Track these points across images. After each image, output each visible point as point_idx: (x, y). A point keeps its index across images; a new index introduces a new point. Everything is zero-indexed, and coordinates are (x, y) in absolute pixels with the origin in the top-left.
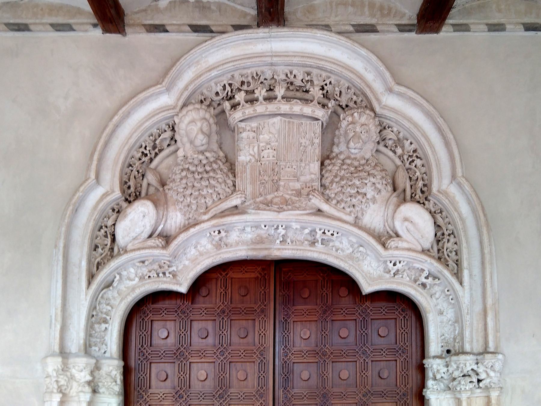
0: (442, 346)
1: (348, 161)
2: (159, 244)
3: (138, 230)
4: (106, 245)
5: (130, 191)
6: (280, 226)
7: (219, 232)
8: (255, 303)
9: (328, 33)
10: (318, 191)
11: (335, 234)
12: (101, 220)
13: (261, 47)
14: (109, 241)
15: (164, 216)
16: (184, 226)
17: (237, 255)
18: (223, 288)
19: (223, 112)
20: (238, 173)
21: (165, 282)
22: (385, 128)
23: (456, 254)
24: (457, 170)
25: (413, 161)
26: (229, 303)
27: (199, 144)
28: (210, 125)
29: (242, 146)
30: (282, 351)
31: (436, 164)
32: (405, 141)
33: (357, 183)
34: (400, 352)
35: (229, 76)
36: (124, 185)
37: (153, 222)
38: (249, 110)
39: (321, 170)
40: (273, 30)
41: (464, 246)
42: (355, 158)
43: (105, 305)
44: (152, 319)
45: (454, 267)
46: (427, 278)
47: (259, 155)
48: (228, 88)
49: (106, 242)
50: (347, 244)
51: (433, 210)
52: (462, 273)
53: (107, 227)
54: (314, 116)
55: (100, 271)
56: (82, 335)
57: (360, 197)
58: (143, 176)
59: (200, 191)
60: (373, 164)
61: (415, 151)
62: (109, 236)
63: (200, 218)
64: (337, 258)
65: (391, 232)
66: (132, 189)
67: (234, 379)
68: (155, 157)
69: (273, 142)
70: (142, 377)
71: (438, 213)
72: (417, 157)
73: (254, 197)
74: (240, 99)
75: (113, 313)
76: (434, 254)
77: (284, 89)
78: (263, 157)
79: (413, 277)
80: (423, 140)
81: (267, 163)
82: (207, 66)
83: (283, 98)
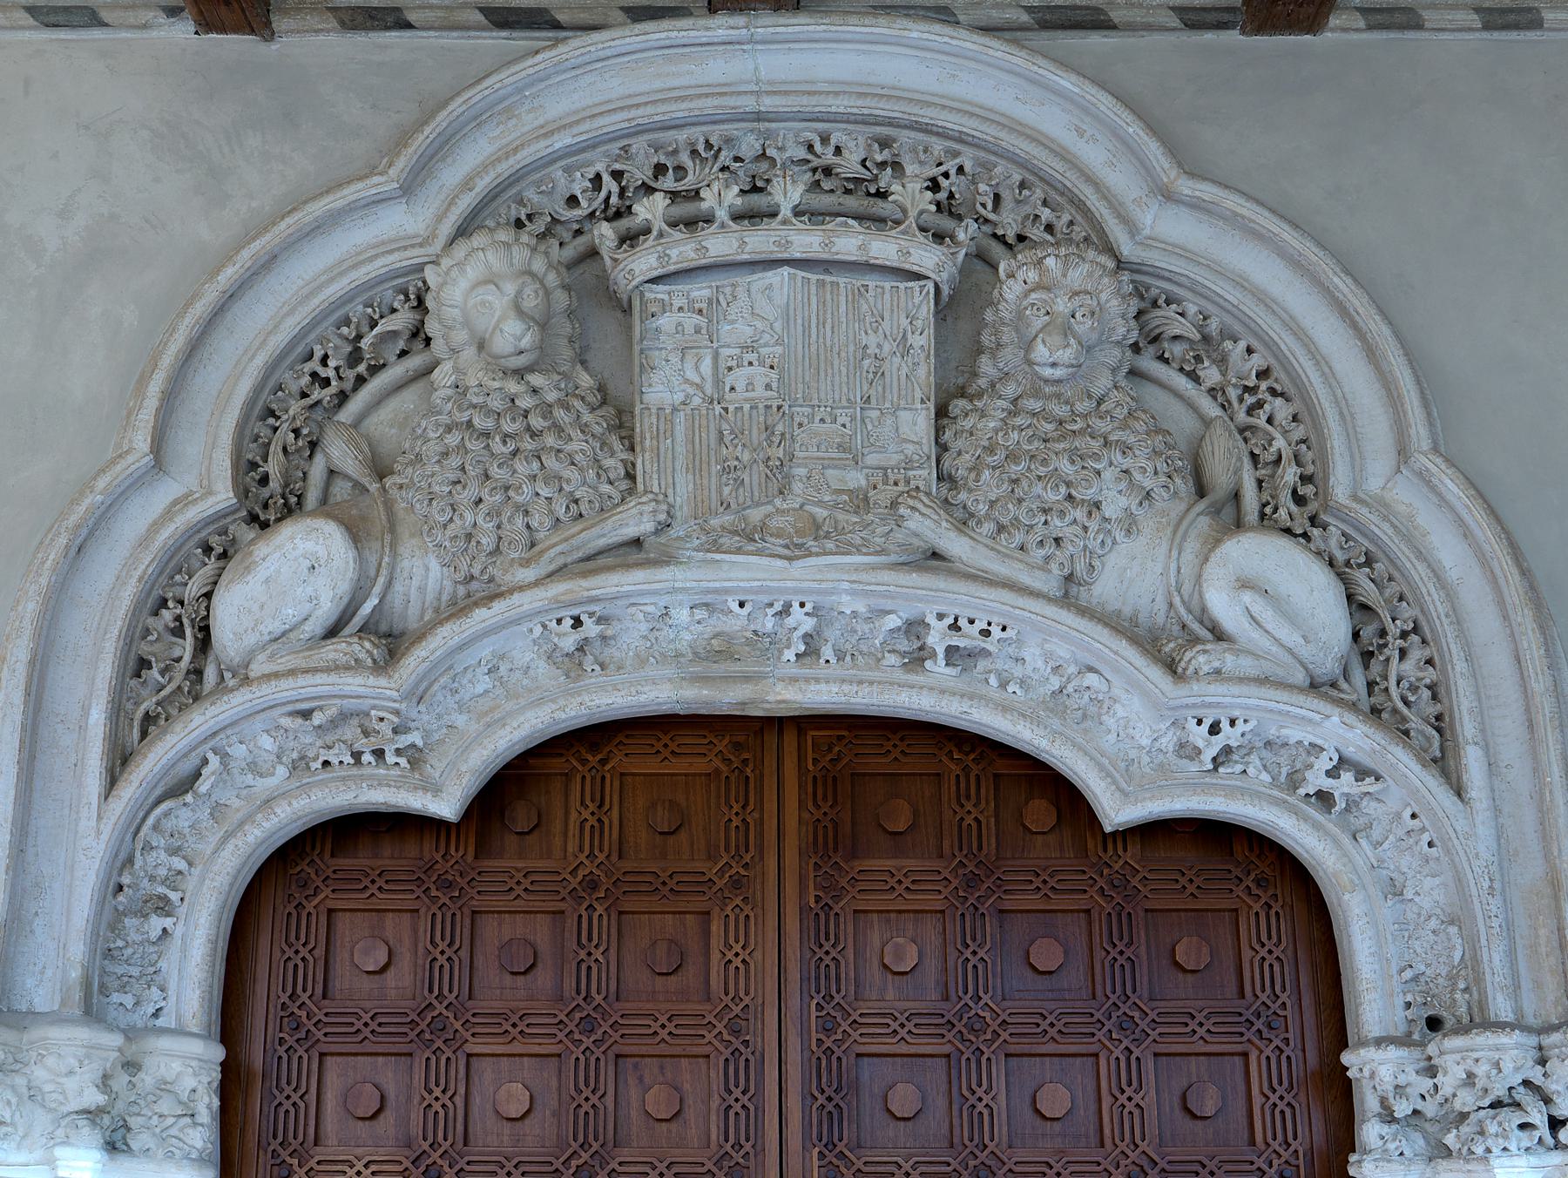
0: (1408, 1005)
1: (1034, 404)
2: (363, 655)
3: (291, 613)
4: (179, 660)
5: (265, 492)
6: (796, 605)
7: (577, 622)
8: (709, 858)
9: (948, 30)
10: (928, 494)
11: (996, 631)
12: (163, 580)
13: (718, 69)
14: (186, 648)
15: (384, 572)
16: (453, 602)
17: (643, 698)
18: (592, 807)
19: (593, 253)
20: (643, 438)
21: (381, 783)
22: (1155, 304)
23: (1435, 697)
24: (1413, 431)
25: (1260, 405)
26: (614, 858)
27: (509, 349)
28: (547, 293)
29: (657, 357)
30: (814, 1014)
31: (1341, 414)
32: (1228, 344)
33: (1066, 467)
34: (1259, 1024)
35: (614, 148)
36: (248, 471)
37: (344, 587)
38: (682, 250)
39: (939, 430)
40: (760, 22)
41: (1458, 668)
42: (1058, 396)
43: (163, 855)
44: (331, 904)
45: (1428, 739)
46: (1330, 774)
47: (718, 382)
48: (609, 184)
49: (177, 653)
50: (1040, 664)
51: (1340, 557)
52: (1458, 757)
53: (182, 603)
54: (907, 267)
55: (152, 743)
56: (77, 950)
57: (1079, 514)
58: (313, 445)
59: (511, 493)
60: (1120, 413)
61: (1263, 374)
62: (188, 632)
63: (508, 577)
64: (1005, 709)
65: (1195, 626)
66: (275, 484)
67: (634, 1113)
68: (355, 389)
69: (766, 345)
70: (287, 1105)
71: (1359, 566)
72: (1273, 392)
73: (700, 514)
74: (649, 217)
75: (190, 884)
76: (1354, 697)
77: (801, 188)
78: (732, 389)
79: (1284, 771)
80: (1287, 342)
81: (747, 407)
82: (541, 121)
83: (797, 212)
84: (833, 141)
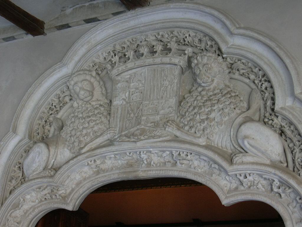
7: (95, 161)
38: (122, 67)
84: (160, 34)
